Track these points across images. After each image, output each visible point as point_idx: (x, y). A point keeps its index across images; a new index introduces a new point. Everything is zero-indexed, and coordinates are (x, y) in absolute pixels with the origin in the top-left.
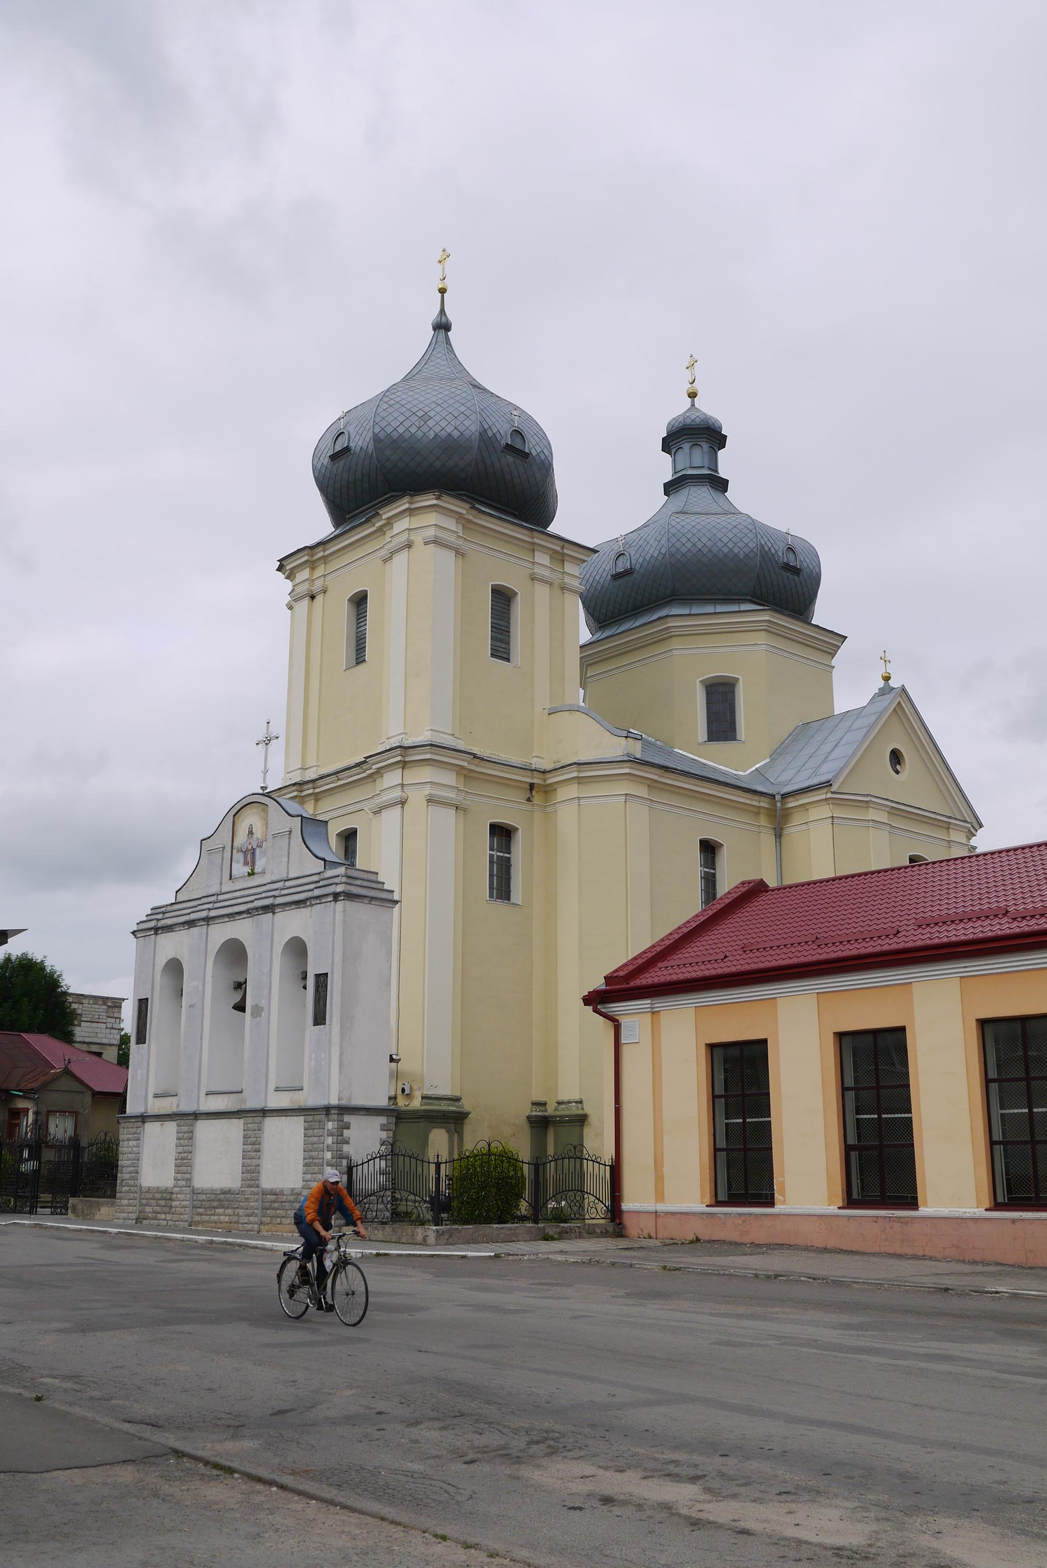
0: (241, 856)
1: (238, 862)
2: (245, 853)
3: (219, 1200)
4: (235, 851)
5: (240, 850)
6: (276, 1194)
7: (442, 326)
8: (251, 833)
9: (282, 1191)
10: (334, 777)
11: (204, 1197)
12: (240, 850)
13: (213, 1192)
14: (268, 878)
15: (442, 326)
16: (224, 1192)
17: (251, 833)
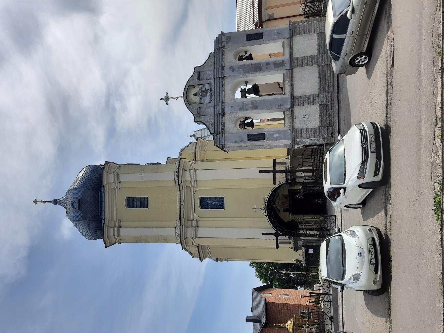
0: (204, 98)
1: (205, 100)
2: (202, 96)
3: (323, 78)
4: (201, 102)
5: (201, 101)
6: (319, 47)
7: (55, 202)
8: (196, 95)
9: (318, 44)
10: (182, 206)
11: (322, 87)
12: (201, 101)
13: (320, 82)
14: (212, 81)
15: (55, 202)
16: (319, 76)
17: (196, 95)
